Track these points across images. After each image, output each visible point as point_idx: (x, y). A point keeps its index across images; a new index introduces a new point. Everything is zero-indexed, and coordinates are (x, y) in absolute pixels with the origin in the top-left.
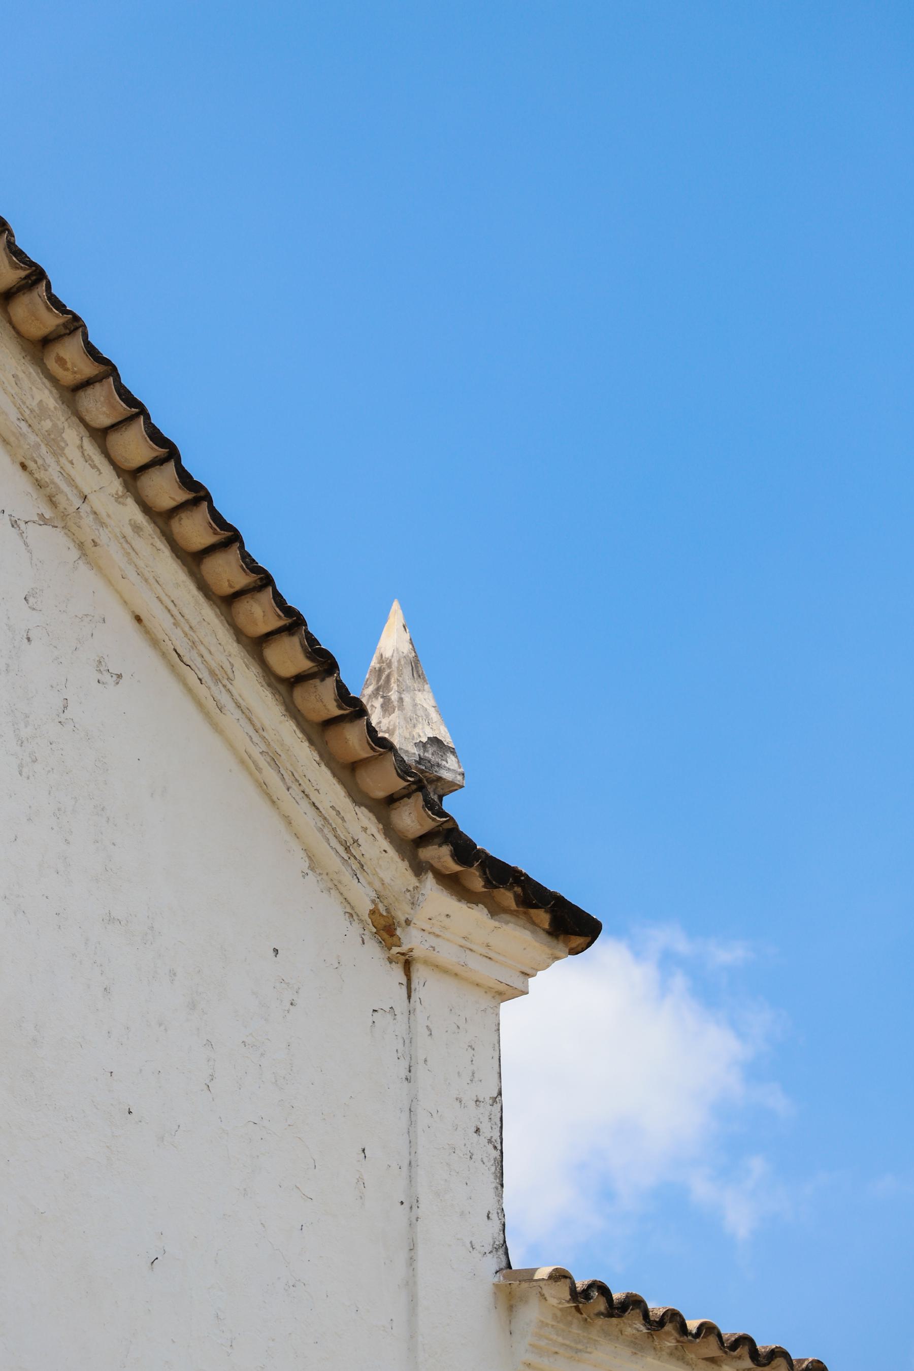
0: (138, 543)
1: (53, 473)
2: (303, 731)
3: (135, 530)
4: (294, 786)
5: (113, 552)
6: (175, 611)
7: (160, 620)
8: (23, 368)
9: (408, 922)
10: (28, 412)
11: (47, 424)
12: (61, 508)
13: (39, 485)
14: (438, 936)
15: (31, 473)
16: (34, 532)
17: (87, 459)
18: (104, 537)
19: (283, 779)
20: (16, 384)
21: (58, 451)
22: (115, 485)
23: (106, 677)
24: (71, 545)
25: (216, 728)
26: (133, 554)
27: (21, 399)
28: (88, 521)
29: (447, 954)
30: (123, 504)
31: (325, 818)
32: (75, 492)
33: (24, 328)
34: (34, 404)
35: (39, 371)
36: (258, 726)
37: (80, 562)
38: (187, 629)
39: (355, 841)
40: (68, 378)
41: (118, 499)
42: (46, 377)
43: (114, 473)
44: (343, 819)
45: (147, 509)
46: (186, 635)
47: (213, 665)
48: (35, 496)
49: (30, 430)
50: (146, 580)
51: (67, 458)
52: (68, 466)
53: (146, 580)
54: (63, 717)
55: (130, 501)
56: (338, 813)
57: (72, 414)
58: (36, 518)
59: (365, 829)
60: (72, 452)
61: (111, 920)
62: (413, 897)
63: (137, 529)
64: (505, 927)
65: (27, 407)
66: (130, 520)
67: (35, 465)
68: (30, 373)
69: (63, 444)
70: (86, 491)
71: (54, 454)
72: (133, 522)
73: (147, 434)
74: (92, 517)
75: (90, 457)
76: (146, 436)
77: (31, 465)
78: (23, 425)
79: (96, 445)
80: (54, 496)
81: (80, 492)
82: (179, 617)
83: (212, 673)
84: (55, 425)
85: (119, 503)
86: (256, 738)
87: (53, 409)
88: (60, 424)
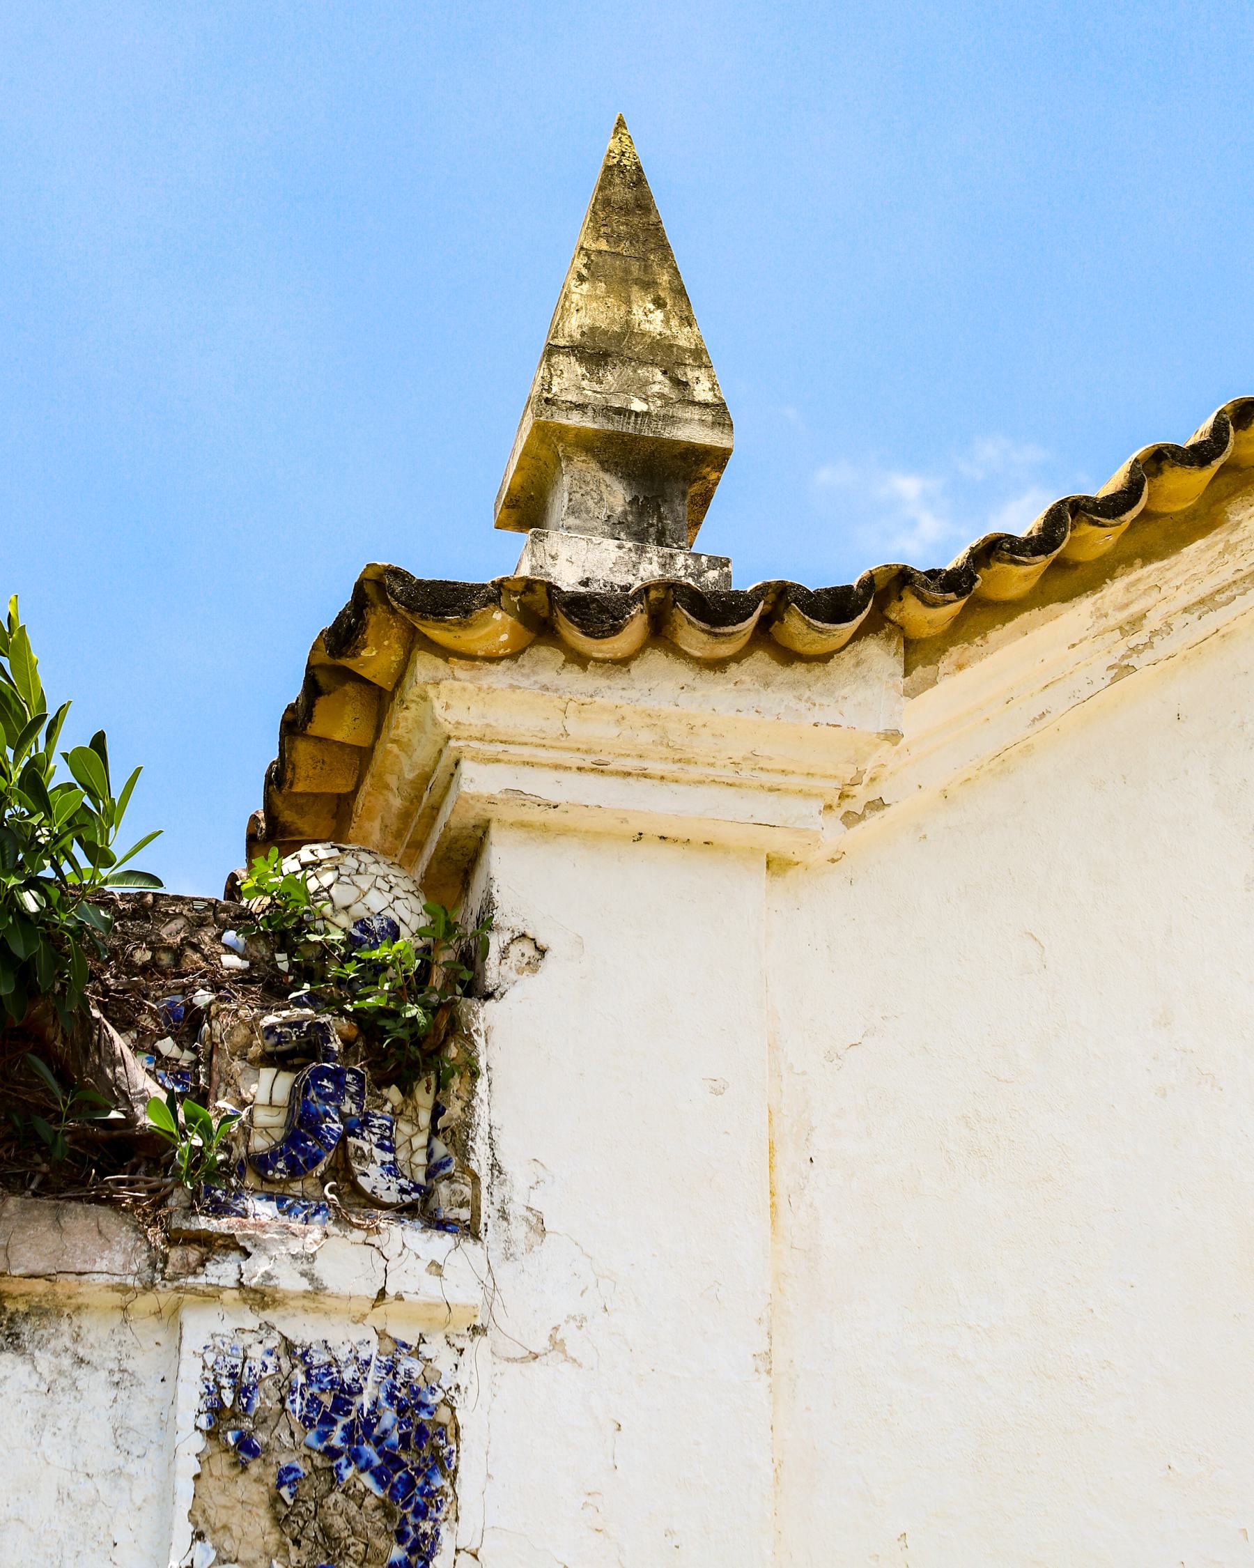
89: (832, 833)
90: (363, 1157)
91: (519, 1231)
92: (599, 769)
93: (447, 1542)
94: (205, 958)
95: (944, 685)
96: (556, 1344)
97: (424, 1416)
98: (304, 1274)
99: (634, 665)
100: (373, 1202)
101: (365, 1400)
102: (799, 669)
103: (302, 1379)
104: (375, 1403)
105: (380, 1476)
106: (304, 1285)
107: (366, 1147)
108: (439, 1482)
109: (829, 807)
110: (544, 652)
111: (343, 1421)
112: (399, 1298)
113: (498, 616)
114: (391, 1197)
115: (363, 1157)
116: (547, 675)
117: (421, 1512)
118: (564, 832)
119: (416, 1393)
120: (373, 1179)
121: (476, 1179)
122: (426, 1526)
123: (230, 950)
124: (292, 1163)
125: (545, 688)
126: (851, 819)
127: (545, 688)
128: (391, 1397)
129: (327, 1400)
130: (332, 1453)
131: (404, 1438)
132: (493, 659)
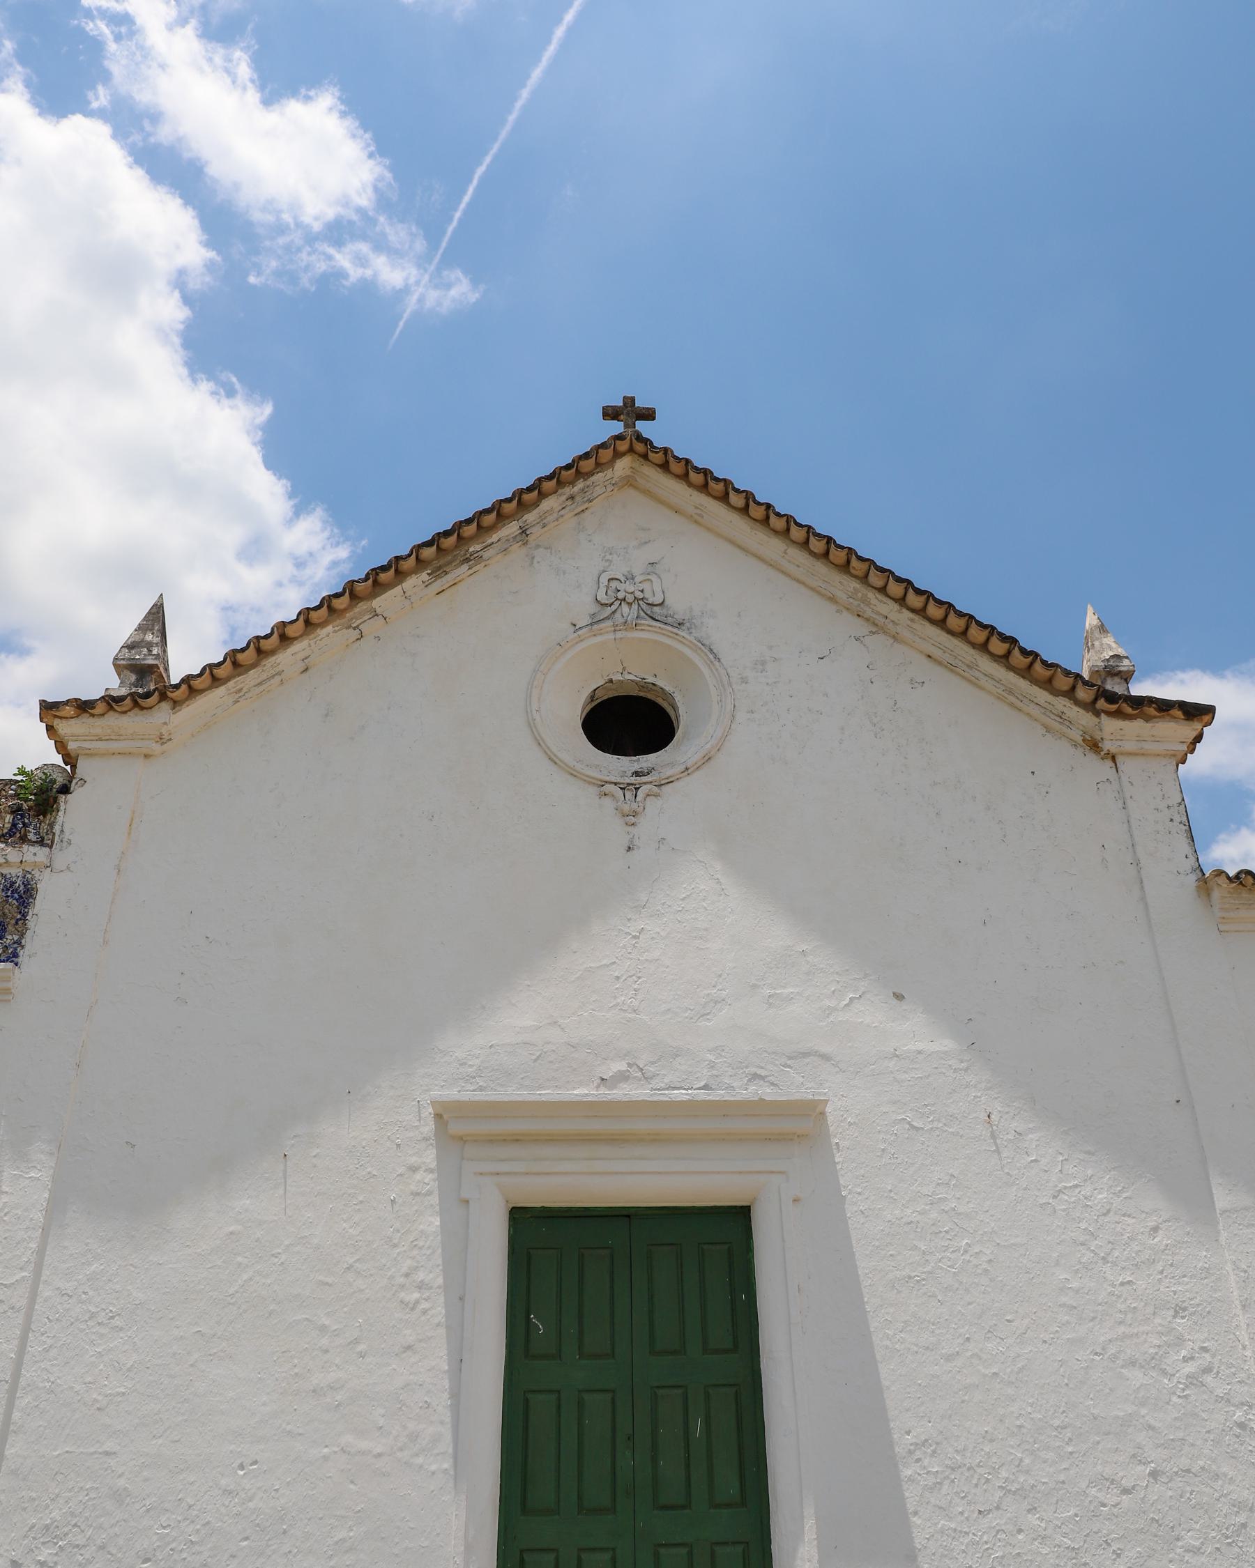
0: (914, 626)
2: (1018, 674)
4: (1025, 700)
5: (906, 634)
6: (941, 647)
7: (937, 653)
9: (1102, 739)
11: (860, 595)
12: (879, 625)
13: (868, 620)
14: (1122, 740)
16: (868, 640)
17: (881, 601)
19: (1018, 698)
21: (868, 604)
22: (896, 606)
23: (916, 685)
24: (888, 638)
25: (981, 688)
26: (915, 631)
28: (890, 626)
29: (1129, 746)
31: (1045, 708)
33: (836, 562)
36: (997, 680)
37: (895, 643)
38: (949, 652)
39: (1063, 713)
40: (860, 574)
43: (893, 602)
44: (1053, 705)
45: (913, 611)
46: (951, 655)
47: (967, 662)
48: (866, 625)
50: (924, 639)
52: (875, 608)
53: (924, 639)
55: (904, 610)
56: (1050, 703)
58: (868, 633)
59: (1065, 706)
60: (874, 601)
61: (935, 784)
62: (1100, 727)
63: (912, 620)
64: (1157, 724)
71: (867, 605)
74: (891, 623)
78: (851, 600)
81: (884, 616)
82: (944, 648)
83: (968, 666)
84: (863, 594)
86: (998, 685)
89: (157, 748)
90: (30, 832)
91: (65, 844)
92: (100, 740)
93: (30, 913)
94: (6, 792)
95: (183, 710)
96: (68, 868)
97: (29, 886)
98: (4, 859)
99: (106, 716)
100: (30, 841)
101: (17, 885)
102: (145, 710)
103: (3, 881)
104: (19, 885)
105: (17, 900)
106: (4, 861)
107: (30, 829)
108: (31, 900)
109: (158, 742)
110: (85, 714)
111: (11, 889)
112: (26, 861)
113: (68, 708)
114: (34, 840)
115: (30, 832)
116: (84, 720)
117: (26, 907)
118: (96, 755)
119: (28, 882)
120: (32, 837)
121: (54, 834)
122: (26, 910)
123: (12, 790)
124: (10, 835)
125: (83, 723)
126: (163, 744)
127: (83, 723)
128: (23, 883)
129: (8, 885)
130: (8, 896)
131: (24, 892)
132: (72, 718)
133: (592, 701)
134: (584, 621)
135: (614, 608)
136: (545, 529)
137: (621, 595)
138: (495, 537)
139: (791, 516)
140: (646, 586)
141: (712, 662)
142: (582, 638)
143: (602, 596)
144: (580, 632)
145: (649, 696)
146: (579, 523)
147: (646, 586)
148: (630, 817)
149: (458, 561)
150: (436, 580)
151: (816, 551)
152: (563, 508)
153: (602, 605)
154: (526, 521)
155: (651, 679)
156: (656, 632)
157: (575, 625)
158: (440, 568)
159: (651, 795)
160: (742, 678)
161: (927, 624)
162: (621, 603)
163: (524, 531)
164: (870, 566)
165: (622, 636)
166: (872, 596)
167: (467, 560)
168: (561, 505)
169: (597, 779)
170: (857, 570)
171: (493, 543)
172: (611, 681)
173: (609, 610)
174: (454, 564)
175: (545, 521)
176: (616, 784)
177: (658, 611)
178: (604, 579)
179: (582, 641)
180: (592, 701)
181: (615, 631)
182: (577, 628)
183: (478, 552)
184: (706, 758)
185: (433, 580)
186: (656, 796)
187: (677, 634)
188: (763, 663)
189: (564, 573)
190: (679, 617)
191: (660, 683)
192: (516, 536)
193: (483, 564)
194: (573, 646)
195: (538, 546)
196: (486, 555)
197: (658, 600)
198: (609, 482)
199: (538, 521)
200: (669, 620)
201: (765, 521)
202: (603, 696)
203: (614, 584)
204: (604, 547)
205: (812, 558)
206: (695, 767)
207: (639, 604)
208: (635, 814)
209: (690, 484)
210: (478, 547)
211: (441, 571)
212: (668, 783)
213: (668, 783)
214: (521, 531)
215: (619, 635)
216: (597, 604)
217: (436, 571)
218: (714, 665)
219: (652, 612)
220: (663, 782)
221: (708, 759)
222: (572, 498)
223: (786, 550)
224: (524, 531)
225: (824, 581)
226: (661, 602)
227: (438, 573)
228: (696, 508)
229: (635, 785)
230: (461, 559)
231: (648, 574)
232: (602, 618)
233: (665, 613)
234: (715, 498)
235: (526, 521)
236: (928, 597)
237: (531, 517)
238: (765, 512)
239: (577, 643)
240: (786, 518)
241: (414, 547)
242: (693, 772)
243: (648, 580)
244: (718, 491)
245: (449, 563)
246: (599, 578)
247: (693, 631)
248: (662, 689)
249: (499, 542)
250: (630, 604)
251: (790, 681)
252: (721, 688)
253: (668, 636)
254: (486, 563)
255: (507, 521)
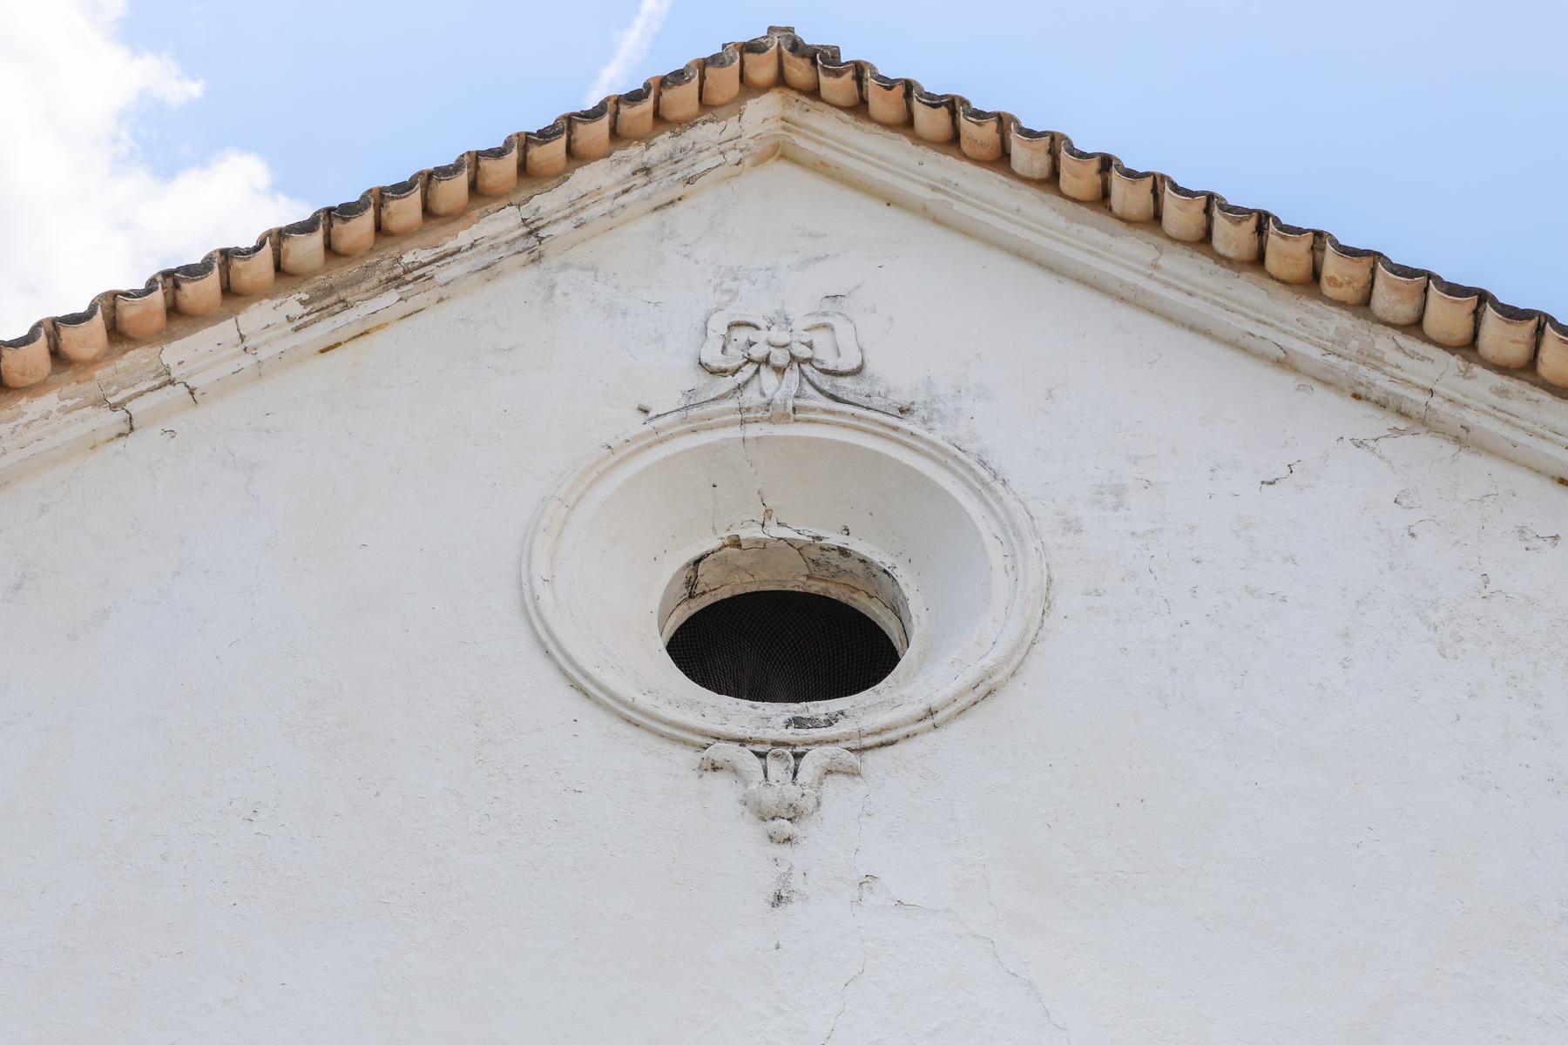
0: (1512, 405)
1: (1382, 383)
3: (1502, 395)
5: (1488, 425)
8: (1303, 309)
10: (1329, 344)
12: (1413, 413)
13: (1381, 405)
15: (1368, 399)
17: (1412, 355)
18: (1470, 417)
20: (1305, 326)
22: (1455, 362)
26: (1513, 419)
27: (1317, 337)
30: (1474, 377)
32: (1418, 391)
33: (1284, 275)
34: (1332, 332)
35: (1321, 303)
37: (1461, 454)
41: (1465, 375)
42: (1331, 305)
45: (1502, 369)
49: (1340, 359)
51: (1392, 365)
53: (1543, 437)
54: (1486, 592)
55: (1477, 370)
57: (1373, 323)
60: (1393, 356)
63: (1502, 392)
65: (1327, 341)
66: (1491, 389)
67: (1364, 388)
68: (1312, 309)
69: (1379, 355)
70: (1429, 385)
71: (1376, 368)
72: (1494, 390)
73: (1442, 292)
75: (1413, 352)
76: (1442, 294)
77: (1361, 390)
79: (1414, 338)
80: (1401, 408)
81: (1424, 389)
85: (1469, 378)
87: (1352, 329)
88: (1366, 338)
133: (691, 596)
134: (666, 400)
135: (740, 378)
136: (582, 232)
137: (758, 352)
138: (464, 238)
139: (1163, 177)
140: (819, 338)
141: (984, 484)
142: (662, 435)
143: (713, 357)
144: (658, 423)
145: (835, 592)
146: (663, 224)
147: (819, 338)
148: (779, 822)
149: (375, 281)
150: (319, 320)
151: (1231, 253)
152: (626, 191)
153: (711, 373)
154: (537, 209)
155: (836, 539)
156: (845, 426)
157: (646, 412)
158: (331, 290)
159: (838, 772)
160: (1066, 522)
161: (1546, 397)
162: (757, 371)
163: (533, 231)
164: (1373, 271)
165: (761, 434)
166: (1385, 343)
167: (396, 281)
168: (619, 183)
169: (693, 731)
170: (1341, 285)
171: (459, 250)
172: (736, 543)
173: (728, 383)
174: (364, 286)
175: (584, 215)
176: (742, 742)
177: (850, 387)
178: (719, 325)
179: (661, 442)
180: (691, 596)
181: (743, 422)
182: (651, 414)
183: (425, 265)
184: (982, 689)
185: (313, 316)
186: (853, 773)
187: (895, 429)
188: (1119, 491)
189: (624, 314)
190: (903, 399)
191: (857, 546)
192: (515, 240)
193: (434, 294)
194: (639, 450)
195: (565, 266)
196: (443, 274)
197: (848, 362)
198: (731, 144)
199: (567, 211)
200: (876, 402)
201: (1102, 199)
202: (720, 586)
203: (742, 335)
204: (720, 267)
205: (1222, 270)
206: (953, 709)
207: (802, 372)
208: (794, 814)
209: (919, 140)
210: (425, 255)
211: (334, 298)
212: (882, 745)
213: (882, 745)
214: (525, 230)
215: (753, 431)
216: (701, 372)
217: (321, 298)
218: (991, 491)
219: (833, 386)
220: (868, 742)
221: (985, 692)
222: (646, 170)
223: (1156, 260)
224: (533, 231)
225: (1259, 321)
226: (855, 365)
227: (326, 302)
228: (935, 189)
229: (795, 746)
230: (384, 277)
231: (825, 314)
232: (712, 396)
233: (867, 391)
234: (978, 162)
235: (537, 209)
236: (1540, 330)
237: (548, 202)
238: (1098, 179)
239: (650, 446)
240: (1149, 180)
241: (269, 234)
242: (948, 720)
243: (825, 326)
244: (982, 145)
245: (354, 282)
246: (706, 323)
247: (937, 425)
248: (863, 561)
249: (474, 250)
250: (780, 370)
251: (1192, 529)
252: (1014, 540)
253: (875, 434)
254: (444, 292)
255: (495, 206)
